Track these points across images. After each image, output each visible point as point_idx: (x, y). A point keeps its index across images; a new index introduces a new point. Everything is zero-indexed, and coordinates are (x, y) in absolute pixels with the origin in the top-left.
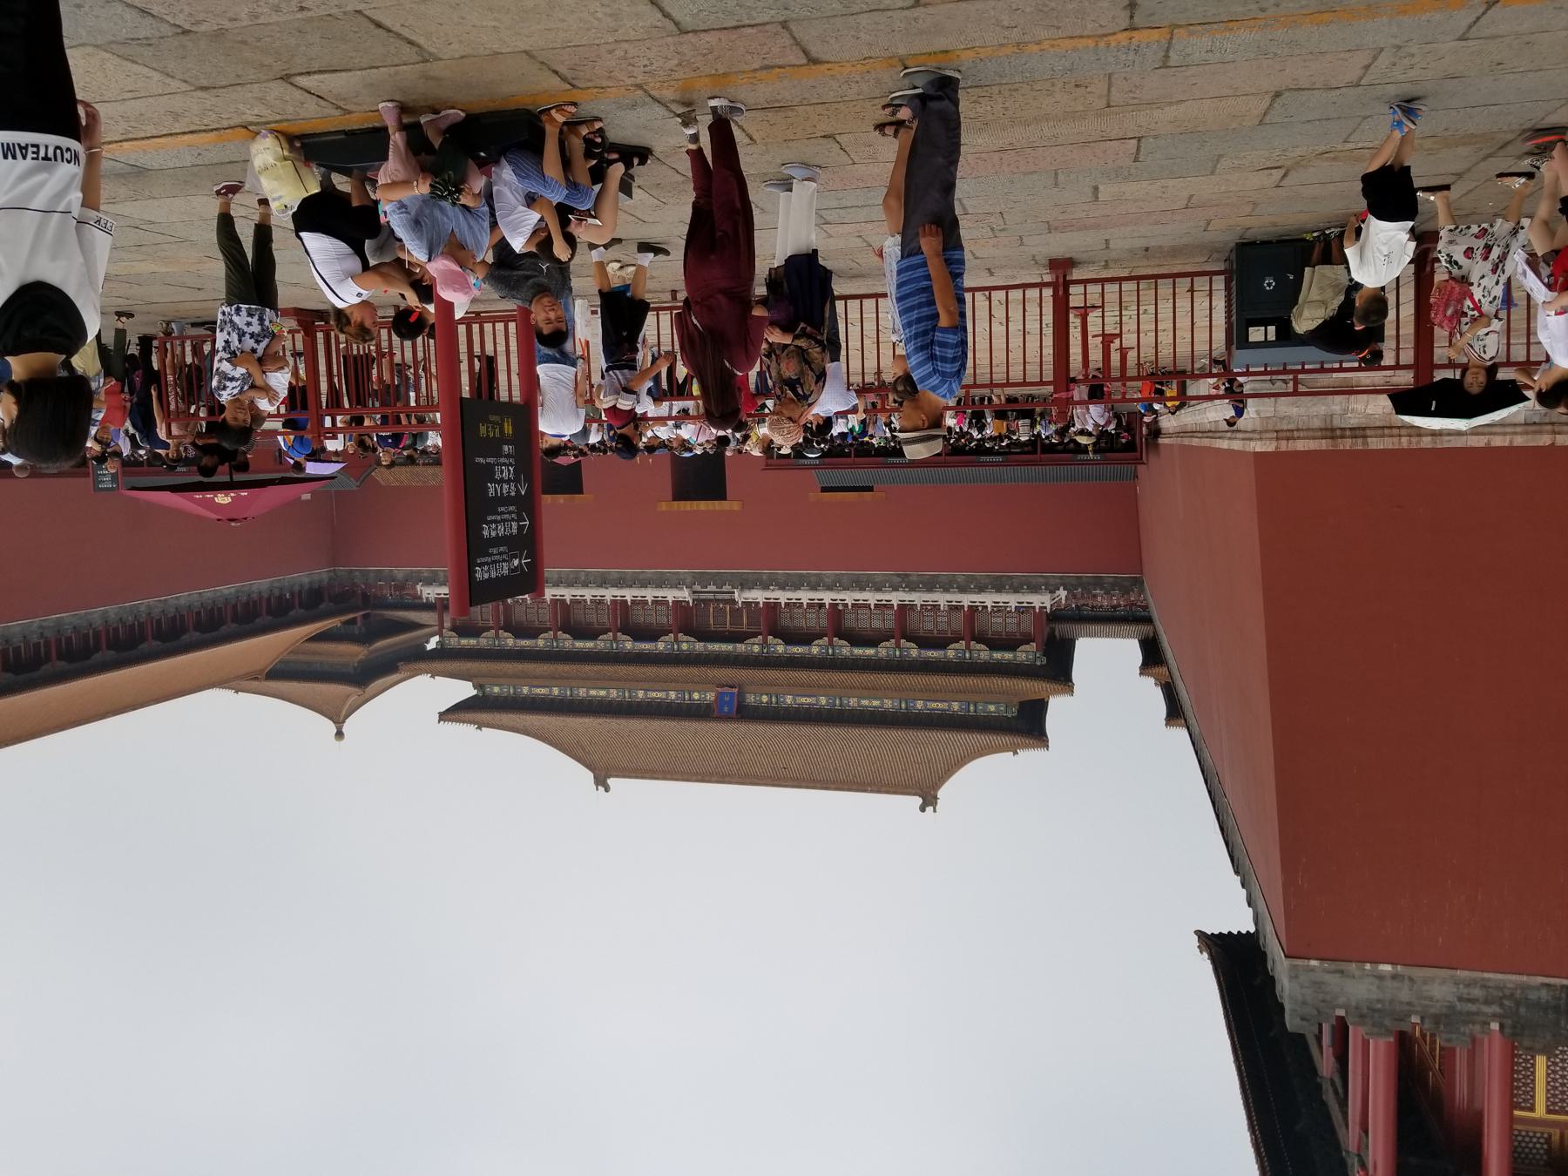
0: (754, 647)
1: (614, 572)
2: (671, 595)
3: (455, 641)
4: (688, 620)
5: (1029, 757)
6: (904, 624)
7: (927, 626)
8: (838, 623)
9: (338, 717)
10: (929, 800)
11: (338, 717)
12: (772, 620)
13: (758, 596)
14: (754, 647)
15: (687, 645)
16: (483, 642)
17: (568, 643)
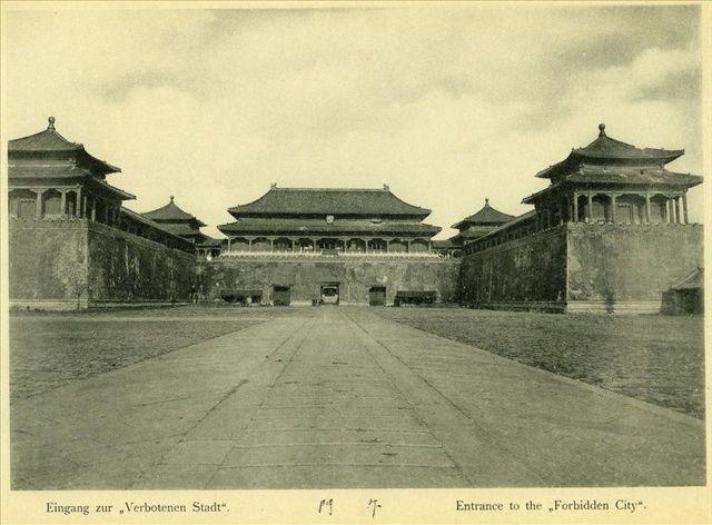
9: (487, 209)
11: (487, 209)
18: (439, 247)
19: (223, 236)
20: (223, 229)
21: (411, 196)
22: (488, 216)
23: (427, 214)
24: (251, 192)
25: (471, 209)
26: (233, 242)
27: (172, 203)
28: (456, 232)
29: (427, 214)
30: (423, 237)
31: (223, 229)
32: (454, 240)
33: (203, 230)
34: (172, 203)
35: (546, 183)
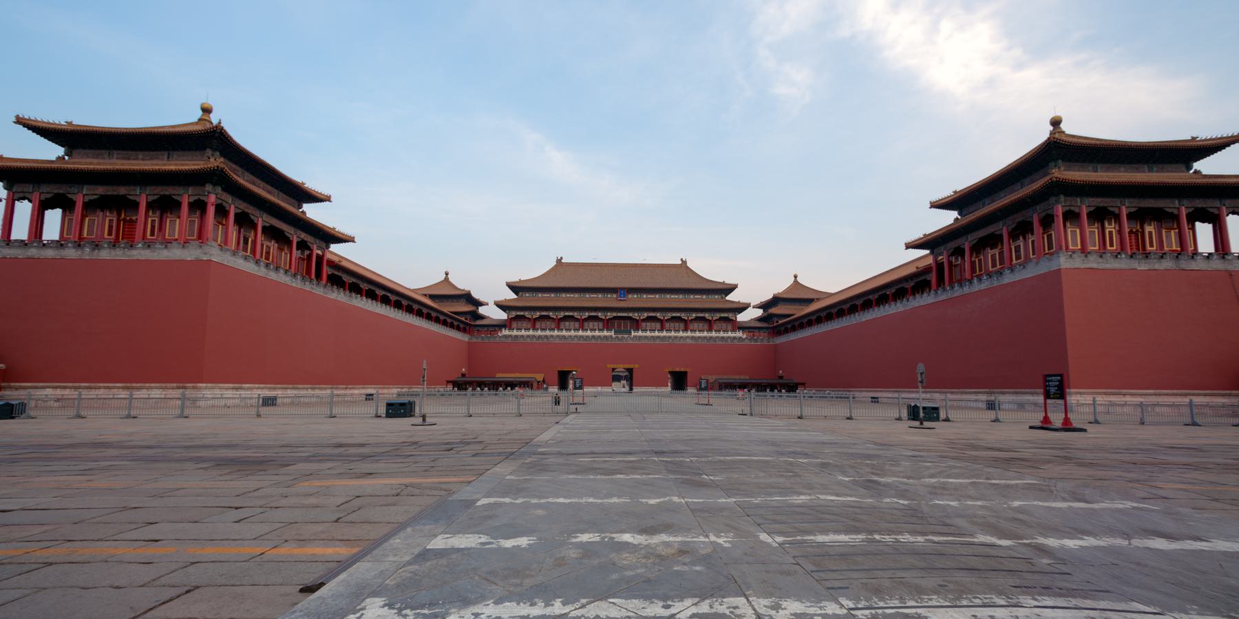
0: (610, 315)
1: (658, 342)
2: (640, 333)
3: (730, 316)
4: (636, 324)
5: (514, 278)
6: (558, 323)
7: (525, 324)
8: (582, 324)
10: (559, 261)
12: (608, 324)
13: (605, 333)
14: (610, 315)
15: (636, 315)
16: (718, 315)
17: (684, 316)
18: (742, 327)
19: (502, 315)
20: (502, 306)
21: (710, 269)
22: (797, 296)
23: (732, 288)
24: (533, 269)
25: (780, 286)
26: (510, 320)
27: (446, 279)
28: (759, 312)
29: (731, 289)
30: (727, 315)
31: (502, 306)
32: (760, 319)
33: (482, 310)
34: (446, 279)
35: (948, 218)
